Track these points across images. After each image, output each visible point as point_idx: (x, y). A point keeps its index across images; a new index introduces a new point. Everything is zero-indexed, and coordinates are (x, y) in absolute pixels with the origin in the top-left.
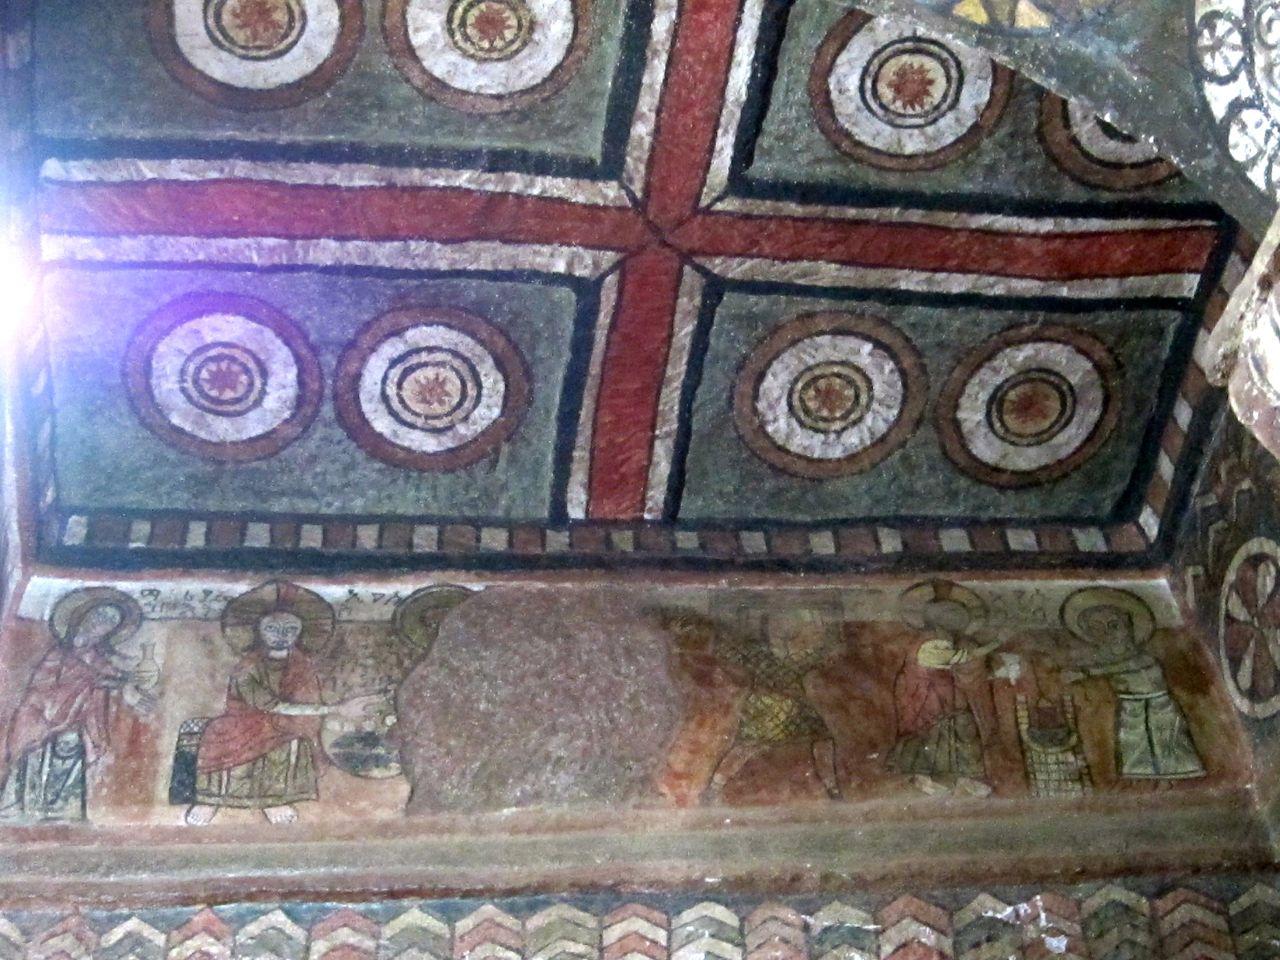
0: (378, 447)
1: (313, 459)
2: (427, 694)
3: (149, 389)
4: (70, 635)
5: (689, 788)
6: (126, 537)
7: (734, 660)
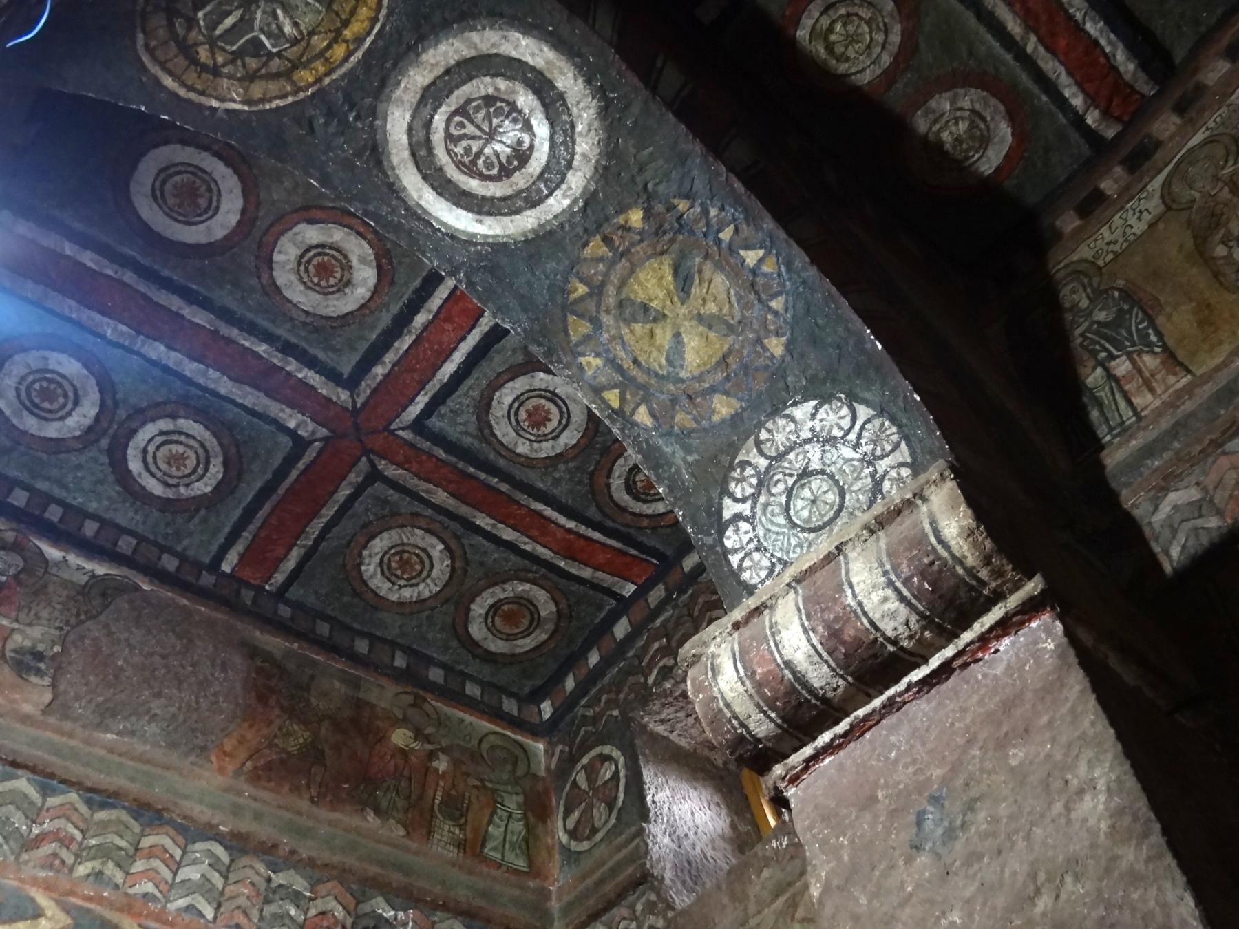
0: (124, 478)
1: (79, 467)
2: (87, 642)
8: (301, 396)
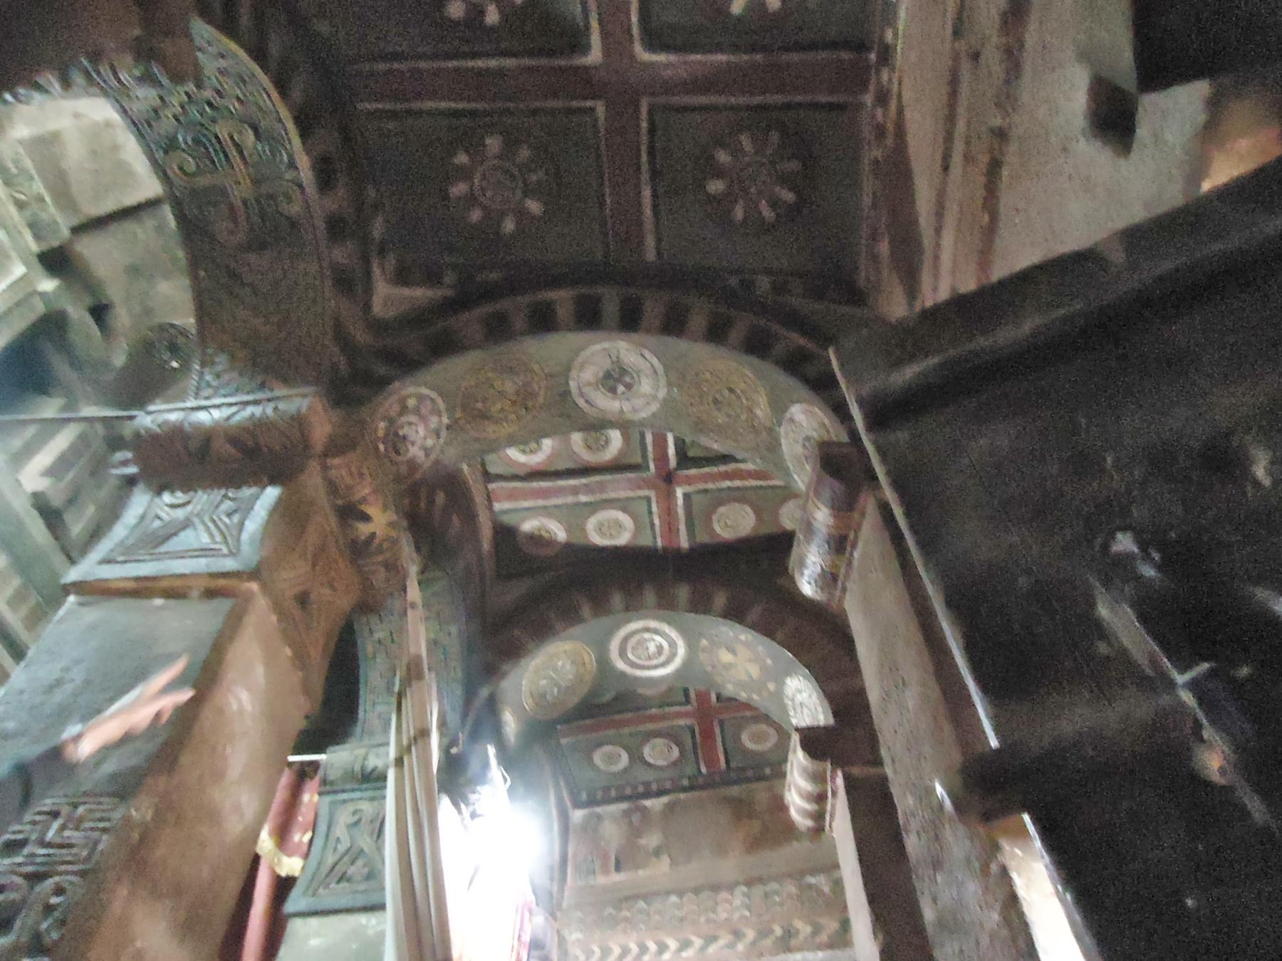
0: (649, 765)
8: (679, 715)
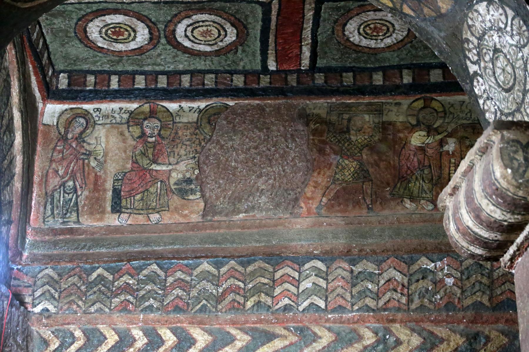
0: (186, 50)
1: (159, 55)
3: (87, 37)
4: (67, 132)
5: (312, 204)
6: (85, 84)
7: (334, 142)
